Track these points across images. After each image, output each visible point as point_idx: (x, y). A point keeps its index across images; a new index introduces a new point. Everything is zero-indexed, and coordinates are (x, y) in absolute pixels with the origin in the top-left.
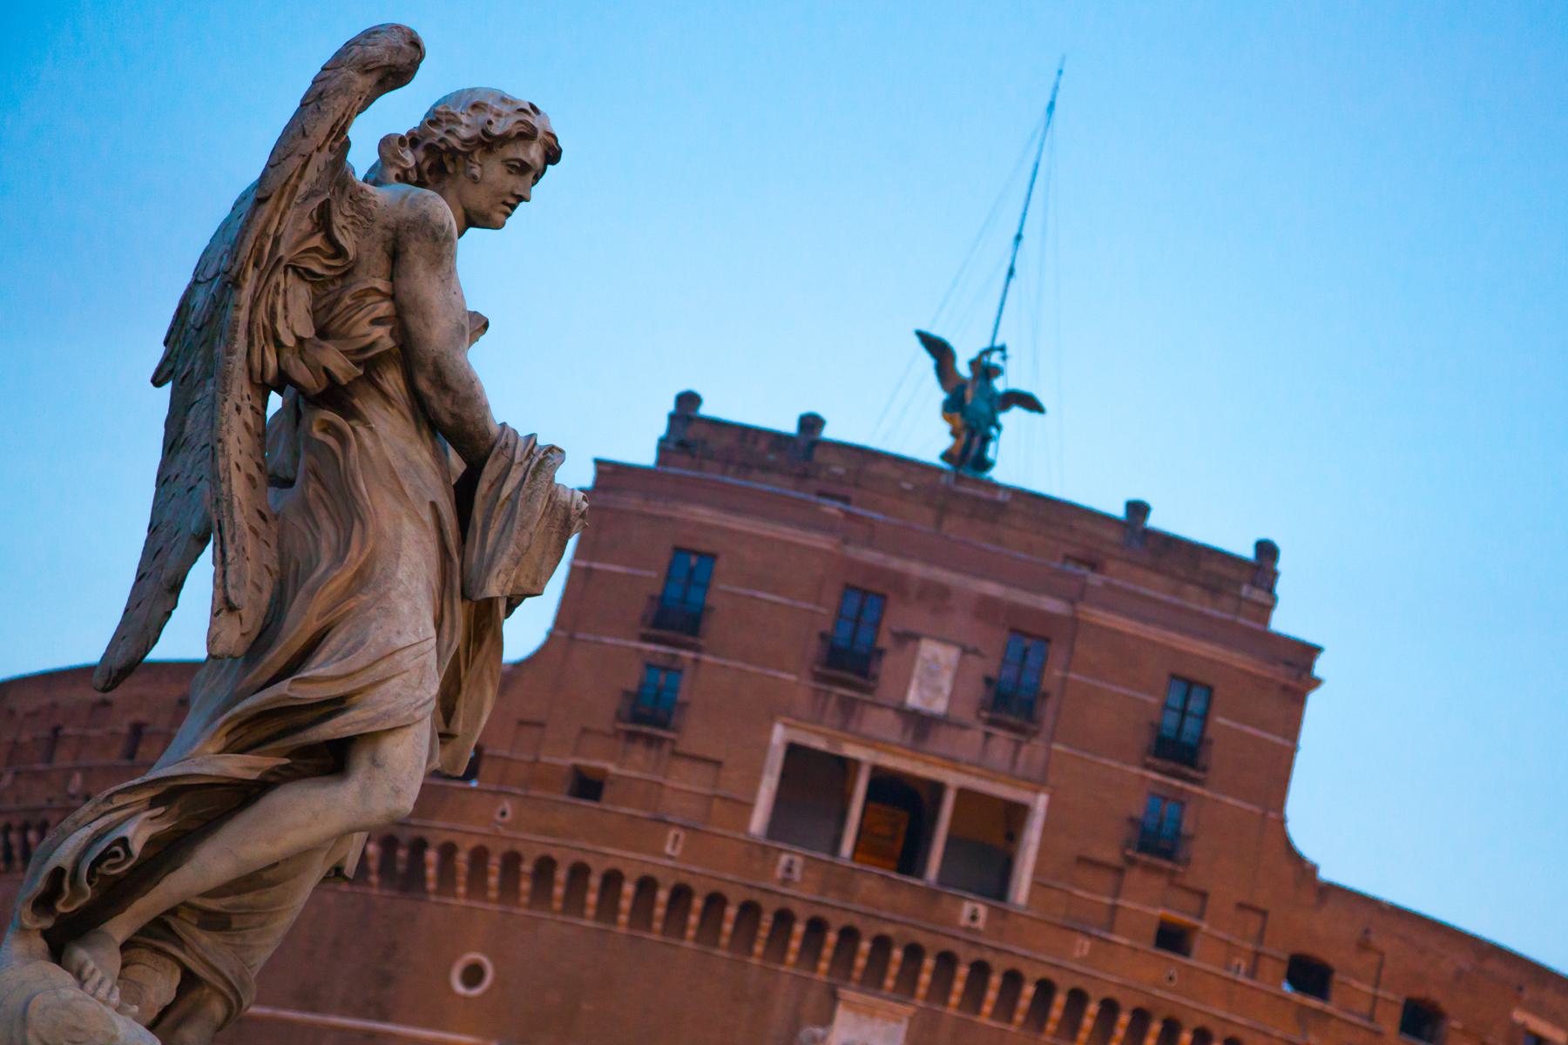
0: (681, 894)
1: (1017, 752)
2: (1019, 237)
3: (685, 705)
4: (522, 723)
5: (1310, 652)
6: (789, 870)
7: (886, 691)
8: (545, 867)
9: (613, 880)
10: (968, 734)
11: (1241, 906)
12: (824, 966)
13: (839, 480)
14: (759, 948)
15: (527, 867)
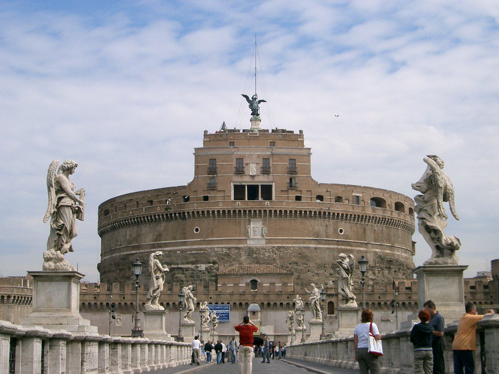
0: (224, 211)
1: (268, 177)
2: (256, 68)
3: (217, 183)
4: (194, 191)
5: (310, 149)
6: (239, 204)
7: (246, 173)
8: (203, 212)
9: (213, 212)
10: (260, 176)
11: (307, 191)
12: (247, 216)
13: (232, 139)
14: (237, 216)
15: (200, 213)
